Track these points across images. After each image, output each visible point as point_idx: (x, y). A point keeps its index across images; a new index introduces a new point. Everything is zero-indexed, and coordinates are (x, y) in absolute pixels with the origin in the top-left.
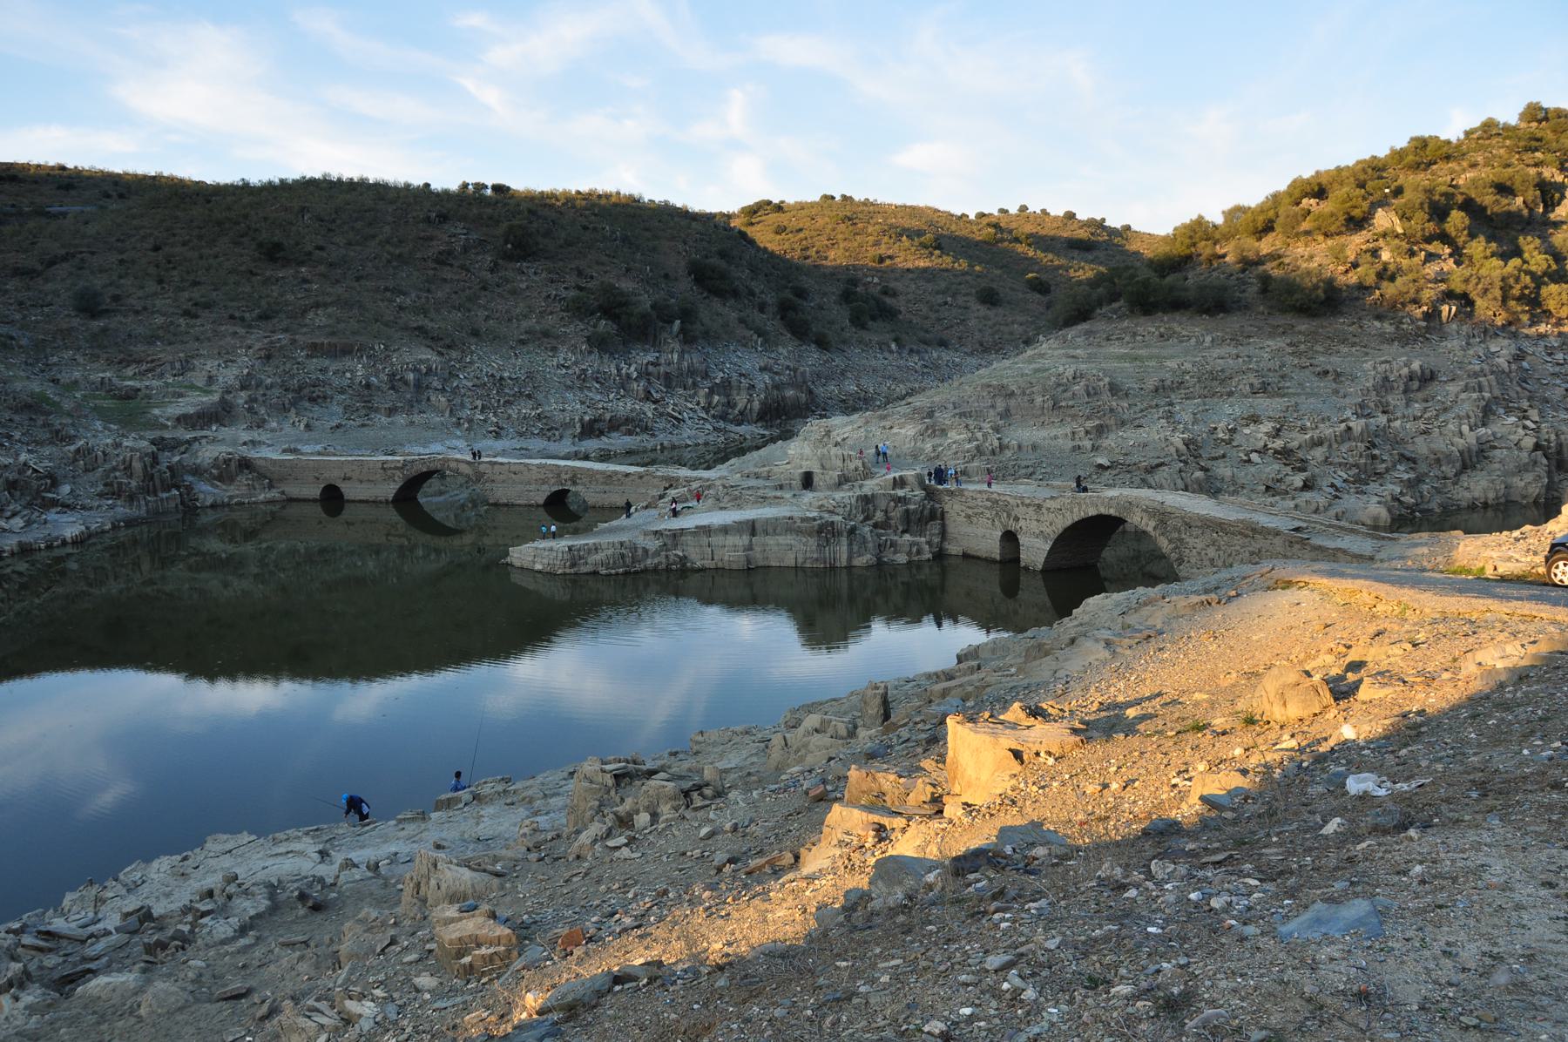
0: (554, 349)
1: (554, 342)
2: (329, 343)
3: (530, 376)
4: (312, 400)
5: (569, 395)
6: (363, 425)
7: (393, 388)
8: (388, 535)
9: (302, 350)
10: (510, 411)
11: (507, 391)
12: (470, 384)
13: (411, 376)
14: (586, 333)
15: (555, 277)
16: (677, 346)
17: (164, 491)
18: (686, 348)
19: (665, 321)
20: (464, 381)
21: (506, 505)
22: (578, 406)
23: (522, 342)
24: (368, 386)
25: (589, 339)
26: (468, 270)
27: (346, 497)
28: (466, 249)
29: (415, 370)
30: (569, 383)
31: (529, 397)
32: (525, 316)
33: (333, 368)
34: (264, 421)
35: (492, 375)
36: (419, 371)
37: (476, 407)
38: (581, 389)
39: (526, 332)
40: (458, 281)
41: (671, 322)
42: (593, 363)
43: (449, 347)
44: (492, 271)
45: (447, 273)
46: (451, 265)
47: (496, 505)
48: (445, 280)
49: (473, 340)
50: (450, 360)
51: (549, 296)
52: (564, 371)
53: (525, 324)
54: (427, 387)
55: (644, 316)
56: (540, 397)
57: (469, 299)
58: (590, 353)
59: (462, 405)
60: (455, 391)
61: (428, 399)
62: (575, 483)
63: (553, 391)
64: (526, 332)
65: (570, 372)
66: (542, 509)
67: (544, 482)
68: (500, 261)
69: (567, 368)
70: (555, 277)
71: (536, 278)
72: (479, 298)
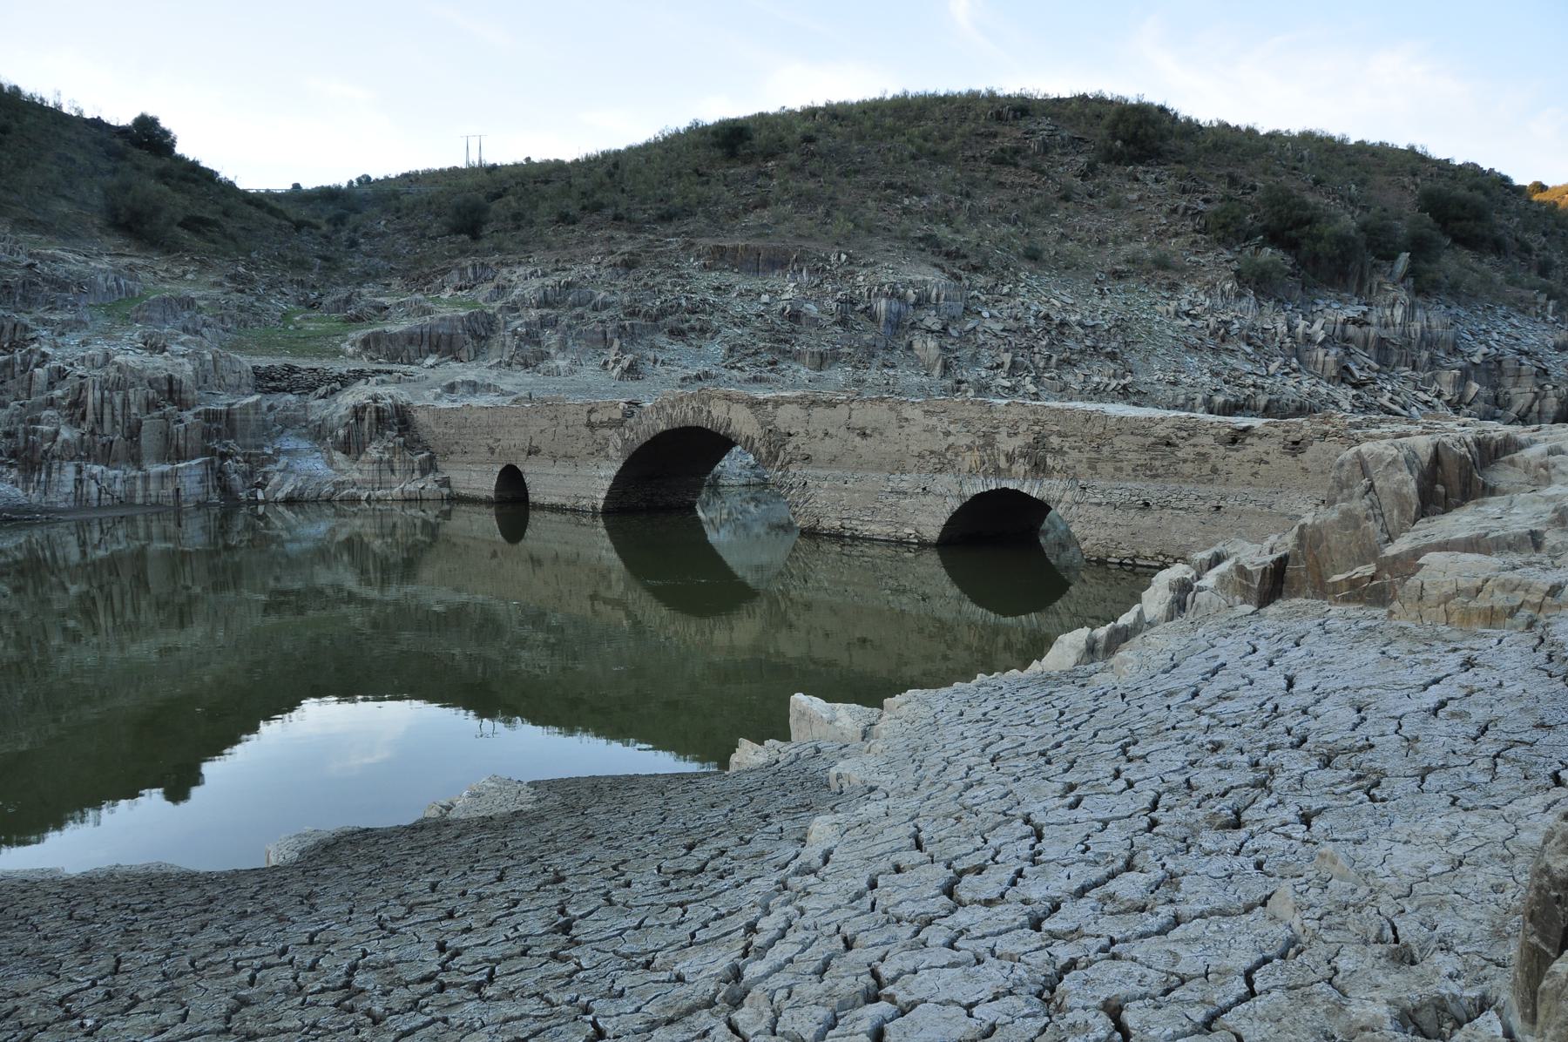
0: (1174, 287)
1: (1175, 277)
2: (746, 248)
3: (1121, 326)
4: (677, 333)
5: (1192, 360)
6: (755, 379)
7: (843, 322)
8: (594, 597)
9: (698, 257)
10: (1069, 378)
11: (1070, 343)
12: (997, 327)
13: (882, 305)
14: (1235, 265)
15: (1189, 184)
16: (1403, 295)
17: (163, 458)
18: (1419, 300)
19: (1379, 257)
20: (990, 321)
21: (837, 536)
22: (1206, 378)
23: (1118, 275)
24: (795, 316)
25: (1238, 274)
26: (1043, 172)
27: (533, 498)
28: (1046, 148)
29: (894, 295)
30: (1194, 340)
31: (1112, 356)
32: (1130, 239)
33: (744, 286)
34: (545, 356)
35: (1047, 317)
36: (902, 298)
37: (999, 366)
38: (1215, 351)
39: (1128, 261)
40: (1023, 186)
41: (1392, 258)
42: (1245, 312)
43: (975, 269)
44: (1084, 177)
45: (1007, 175)
46: (1016, 165)
47: (811, 534)
48: (1001, 185)
49: (1028, 265)
50: (971, 287)
51: (1174, 211)
52: (1188, 321)
53: (1127, 249)
54: (913, 326)
55: (1342, 240)
56: (1134, 359)
57: (1037, 211)
58: (1240, 296)
59: (975, 360)
60: (965, 337)
61: (910, 346)
62: (1039, 468)
63: (1160, 351)
64: (1128, 261)
65: (1199, 324)
66: (932, 559)
67: (943, 462)
68: (1101, 165)
69: (1195, 317)
70: (1189, 184)
71: (1159, 187)
72: (1055, 210)
